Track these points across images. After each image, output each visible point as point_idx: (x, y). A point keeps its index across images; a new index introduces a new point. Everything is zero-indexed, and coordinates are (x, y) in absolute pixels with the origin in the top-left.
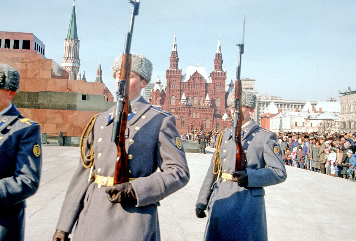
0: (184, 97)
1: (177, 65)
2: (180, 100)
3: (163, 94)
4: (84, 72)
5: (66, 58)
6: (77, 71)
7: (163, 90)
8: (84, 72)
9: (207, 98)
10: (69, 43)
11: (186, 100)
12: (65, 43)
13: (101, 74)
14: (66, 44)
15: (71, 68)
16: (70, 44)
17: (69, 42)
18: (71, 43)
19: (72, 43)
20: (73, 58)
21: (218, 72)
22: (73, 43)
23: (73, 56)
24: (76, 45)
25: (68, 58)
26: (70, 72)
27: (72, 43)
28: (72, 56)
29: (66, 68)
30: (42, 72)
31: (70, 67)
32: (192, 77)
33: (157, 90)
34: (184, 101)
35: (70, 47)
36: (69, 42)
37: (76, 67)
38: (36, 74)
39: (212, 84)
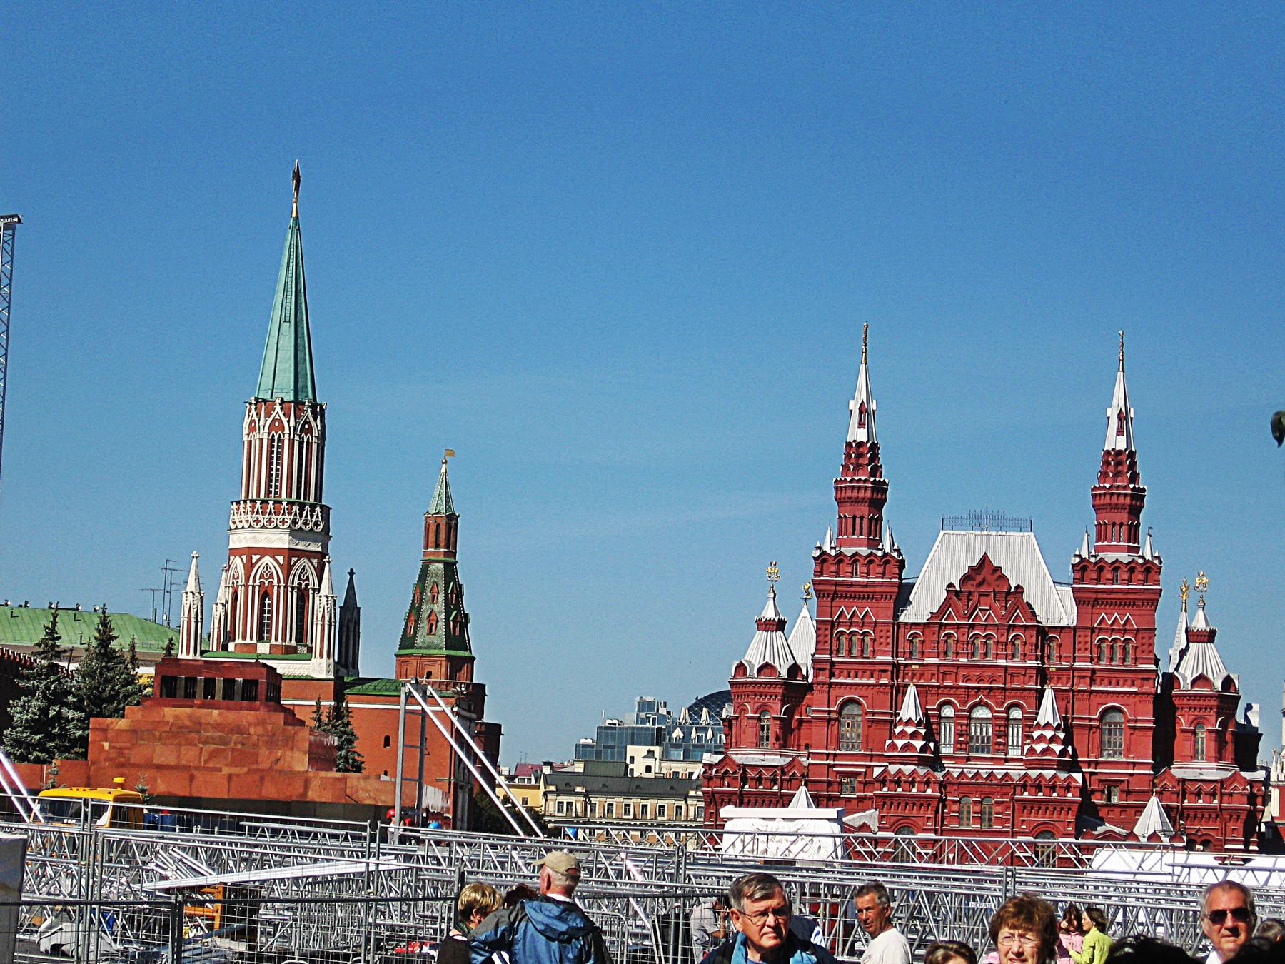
0: (909, 708)
1: (875, 524)
2: (893, 724)
3: (795, 689)
4: (351, 573)
5: (253, 507)
6: (311, 573)
7: (794, 669)
8: (351, 573)
9: (1047, 712)
10: (269, 420)
11: (919, 724)
12: (247, 422)
13: (451, 542)
14: (252, 429)
15: (280, 559)
16: (276, 426)
17: (268, 415)
18: (280, 420)
19: (285, 420)
20: (291, 504)
21: (1110, 557)
22: (289, 424)
23: (289, 494)
24: (310, 430)
25: (264, 502)
26: (275, 582)
27: (285, 420)
28: (284, 496)
29: (255, 558)
30: (288, 753)
31: (273, 552)
32: (958, 593)
33: (766, 667)
34: (910, 730)
35: (274, 446)
36: (268, 415)
37: (310, 555)
38: (278, 760)
39: (1075, 629)
